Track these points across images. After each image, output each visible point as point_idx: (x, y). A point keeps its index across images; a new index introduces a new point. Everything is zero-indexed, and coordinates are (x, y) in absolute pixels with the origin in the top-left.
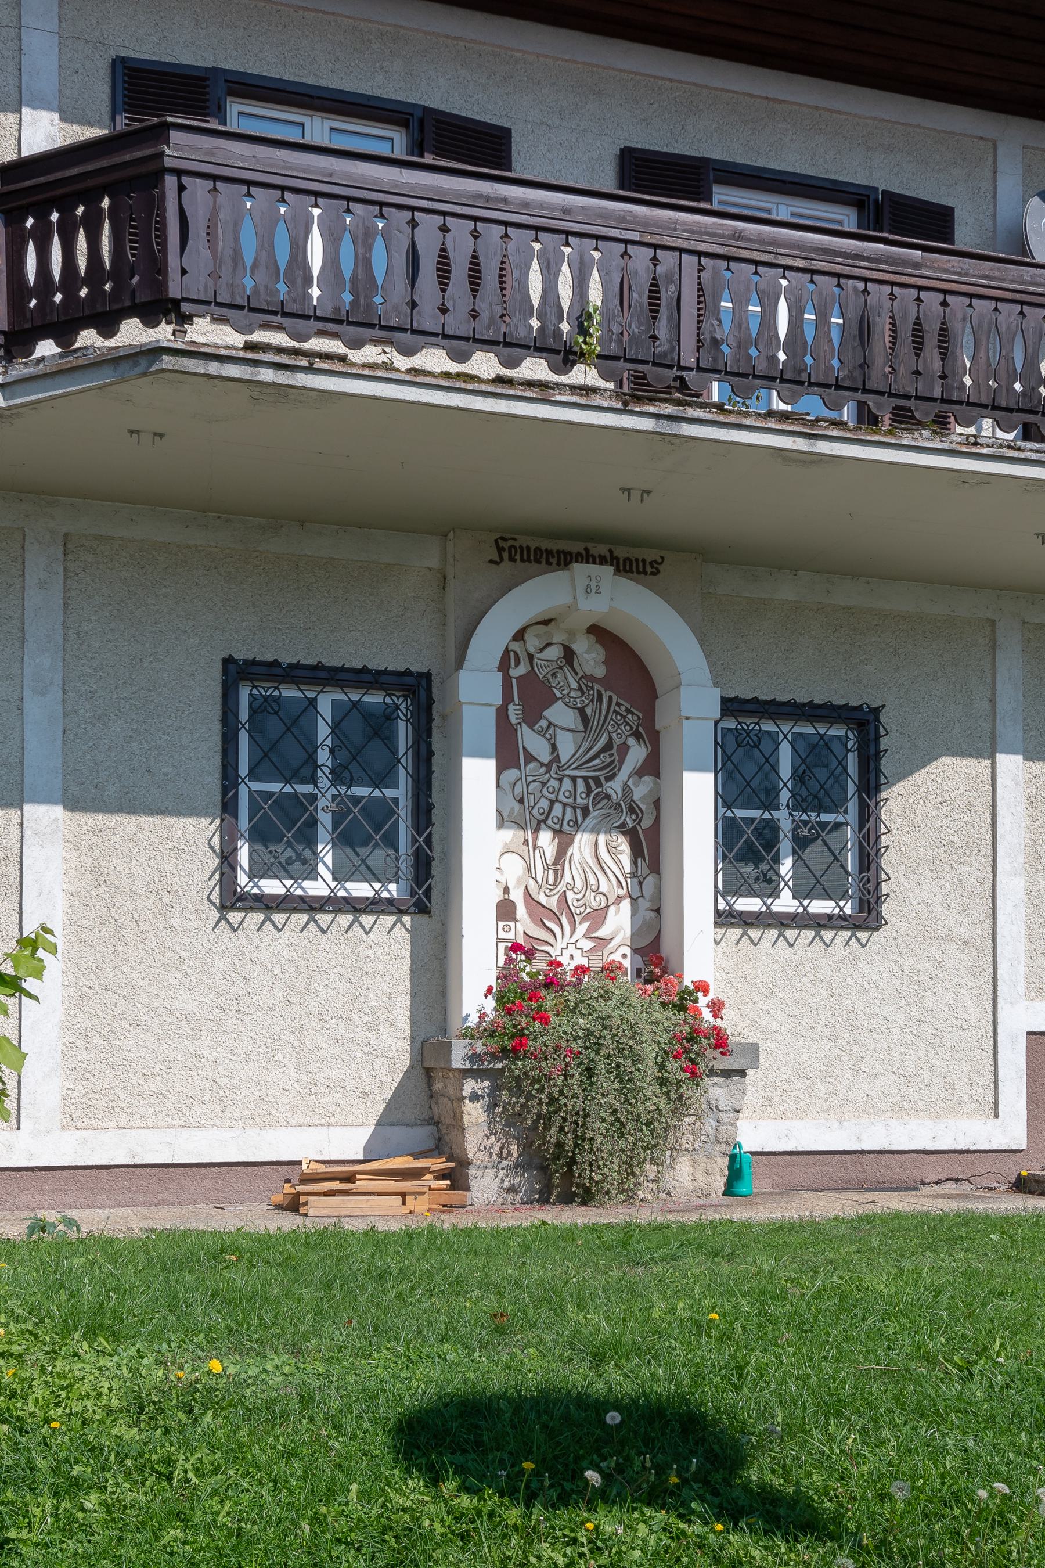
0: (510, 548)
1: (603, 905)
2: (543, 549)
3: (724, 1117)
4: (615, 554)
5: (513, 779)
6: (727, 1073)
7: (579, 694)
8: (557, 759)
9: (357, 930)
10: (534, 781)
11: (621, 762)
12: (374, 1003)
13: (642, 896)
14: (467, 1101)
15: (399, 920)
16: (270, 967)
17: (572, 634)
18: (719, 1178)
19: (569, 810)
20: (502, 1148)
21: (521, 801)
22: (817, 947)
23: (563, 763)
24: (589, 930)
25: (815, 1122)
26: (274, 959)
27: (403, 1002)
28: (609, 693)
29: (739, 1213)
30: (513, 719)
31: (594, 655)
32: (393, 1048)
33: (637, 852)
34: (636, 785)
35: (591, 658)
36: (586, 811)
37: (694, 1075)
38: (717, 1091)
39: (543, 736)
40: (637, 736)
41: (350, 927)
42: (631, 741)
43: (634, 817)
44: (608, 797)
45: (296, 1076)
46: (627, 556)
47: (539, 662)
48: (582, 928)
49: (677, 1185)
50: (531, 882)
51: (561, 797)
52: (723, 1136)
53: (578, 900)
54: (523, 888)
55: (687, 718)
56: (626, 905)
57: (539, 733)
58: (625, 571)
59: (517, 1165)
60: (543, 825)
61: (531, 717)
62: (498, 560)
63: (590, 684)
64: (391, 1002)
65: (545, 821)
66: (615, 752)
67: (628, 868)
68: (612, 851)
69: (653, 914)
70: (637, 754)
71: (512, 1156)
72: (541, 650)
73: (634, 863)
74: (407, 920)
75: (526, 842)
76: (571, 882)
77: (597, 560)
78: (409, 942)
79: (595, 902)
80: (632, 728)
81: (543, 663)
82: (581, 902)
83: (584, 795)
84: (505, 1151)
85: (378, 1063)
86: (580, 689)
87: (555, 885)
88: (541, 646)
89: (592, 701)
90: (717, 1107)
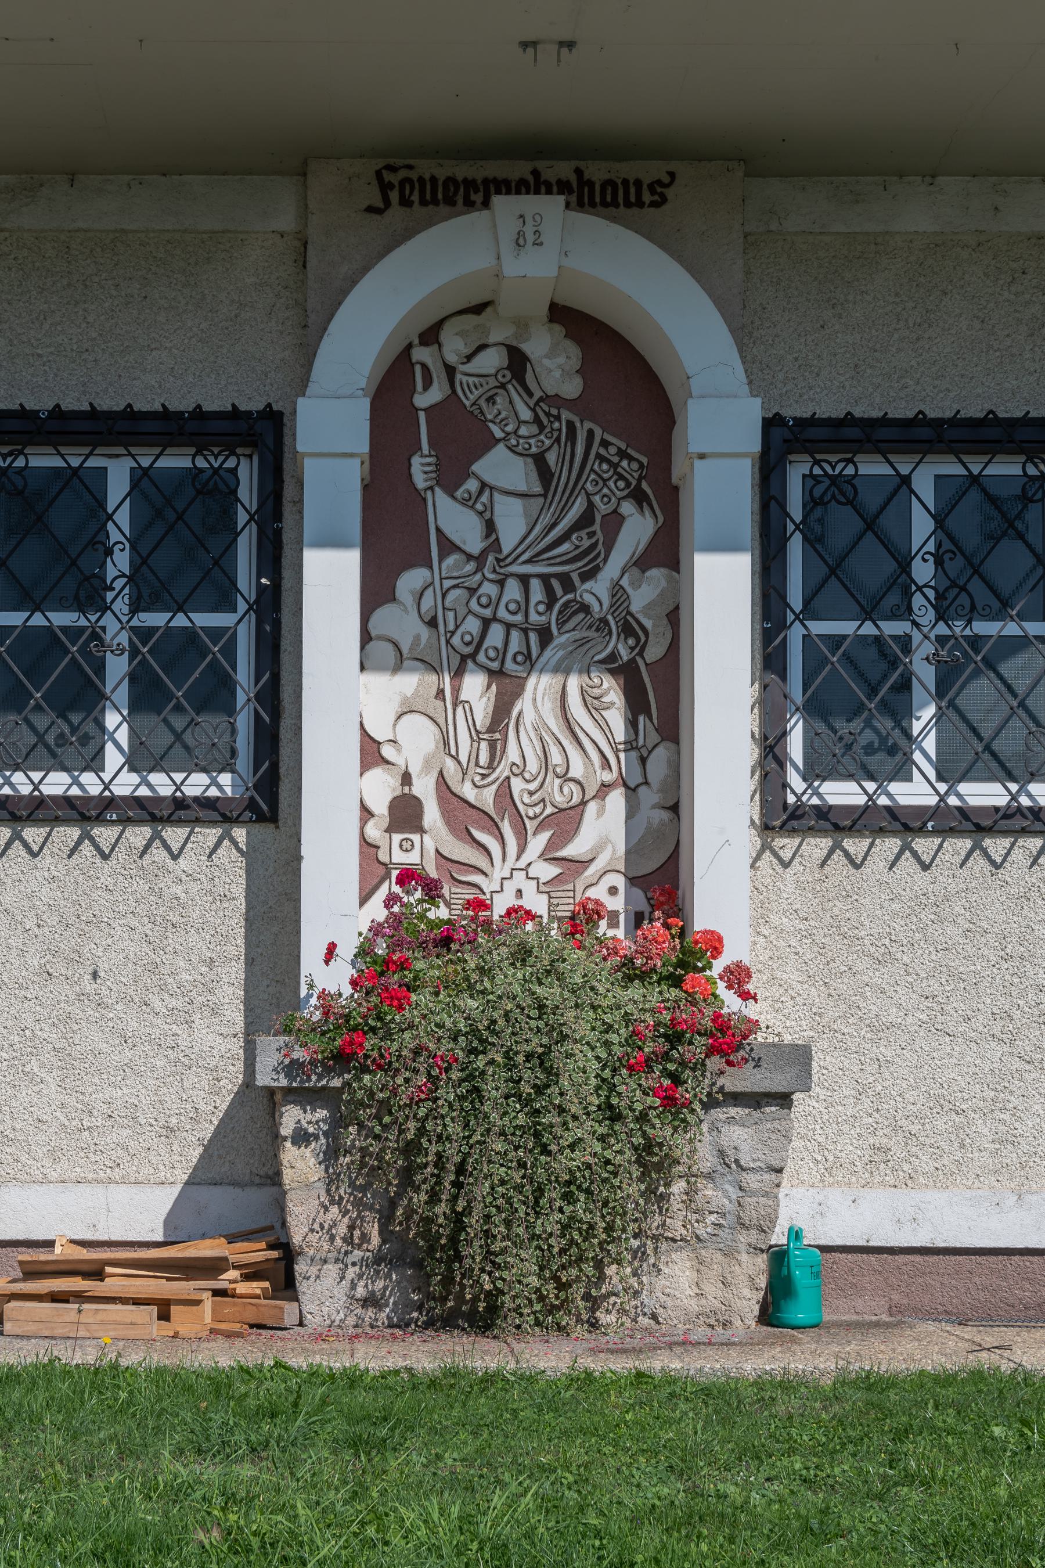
0: (402, 183)
1: (576, 800)
2: (460, 179)
3: (751, 1180)
4: (587, 176)
5: (418, 585)
6: (755, 1100)
7: (535, 430)
8: (495, 546)
9: (158, 853)
10: (455, 587)
11: (609, 547)
12: (185, 976)
13: (646, 783)
14: (288, 1144)
15: (227, 835)
16: (19, 917)
17: (522, 325)
18: (746, 1292)
19: (515, 635)
20: (351, 1228)
21: (432, 623)
22: (977, 869)
23: (506, 550)
24: (551, 845)
25: (969, 1193)
26: (27, 904)
27: (234, 973)
28: (588, 425)
29: (811, 1359)
30: (420, 481)
31: (561, 360)
32: (215, 1052)
33: (636, 704)
34: (636, 585)
35: (556, 366)
36: (545, 637)
37: (669, 1101)
38: (739, 1133)
39: (472, 507)
40: (639, 497)
41: (147, 847)
42: (627, 508)
43: (631, 642)
44: (585, 608)
45: (58, 1098)
46: (607, 176)
47: (465, 379)
48: (537, 843)
49: (669, 1303)
50: (450, 763)
51: (502, 613)
52: (750, 1215)
53: (531, 793)
54: (435, 774)
55: (702, 456)
56: (617, 799)
57: (464, 502)
58: (604, 204)
59: (378, 1260)
60: (470, 664)
61: (451, 475)
62: (381, 205)
63: (554, 412)
64: (212, 975)
65: (473, 656)
66: (597, 529)
67: (620, 735)
68: (592, 704)
69: (665, 815)
70: (638, 529)
71: (369, 1242)
72: (469, 358)
73: (632, 724)
74: (240, 834)
75: (440, 694)
76: (518, 761)
77: (555, 189)
78: (242, 872)
79: (560, 795)
80: (628, 484)
81: (471, 380)
82: (536, 797)
83: (541, 608)
84: (357, 1233)
85: (191, 1078)
86: (537, 420)
87: (491, 766)
88: (468, 351)
89: (558, 440)
90: (737, 1161)
